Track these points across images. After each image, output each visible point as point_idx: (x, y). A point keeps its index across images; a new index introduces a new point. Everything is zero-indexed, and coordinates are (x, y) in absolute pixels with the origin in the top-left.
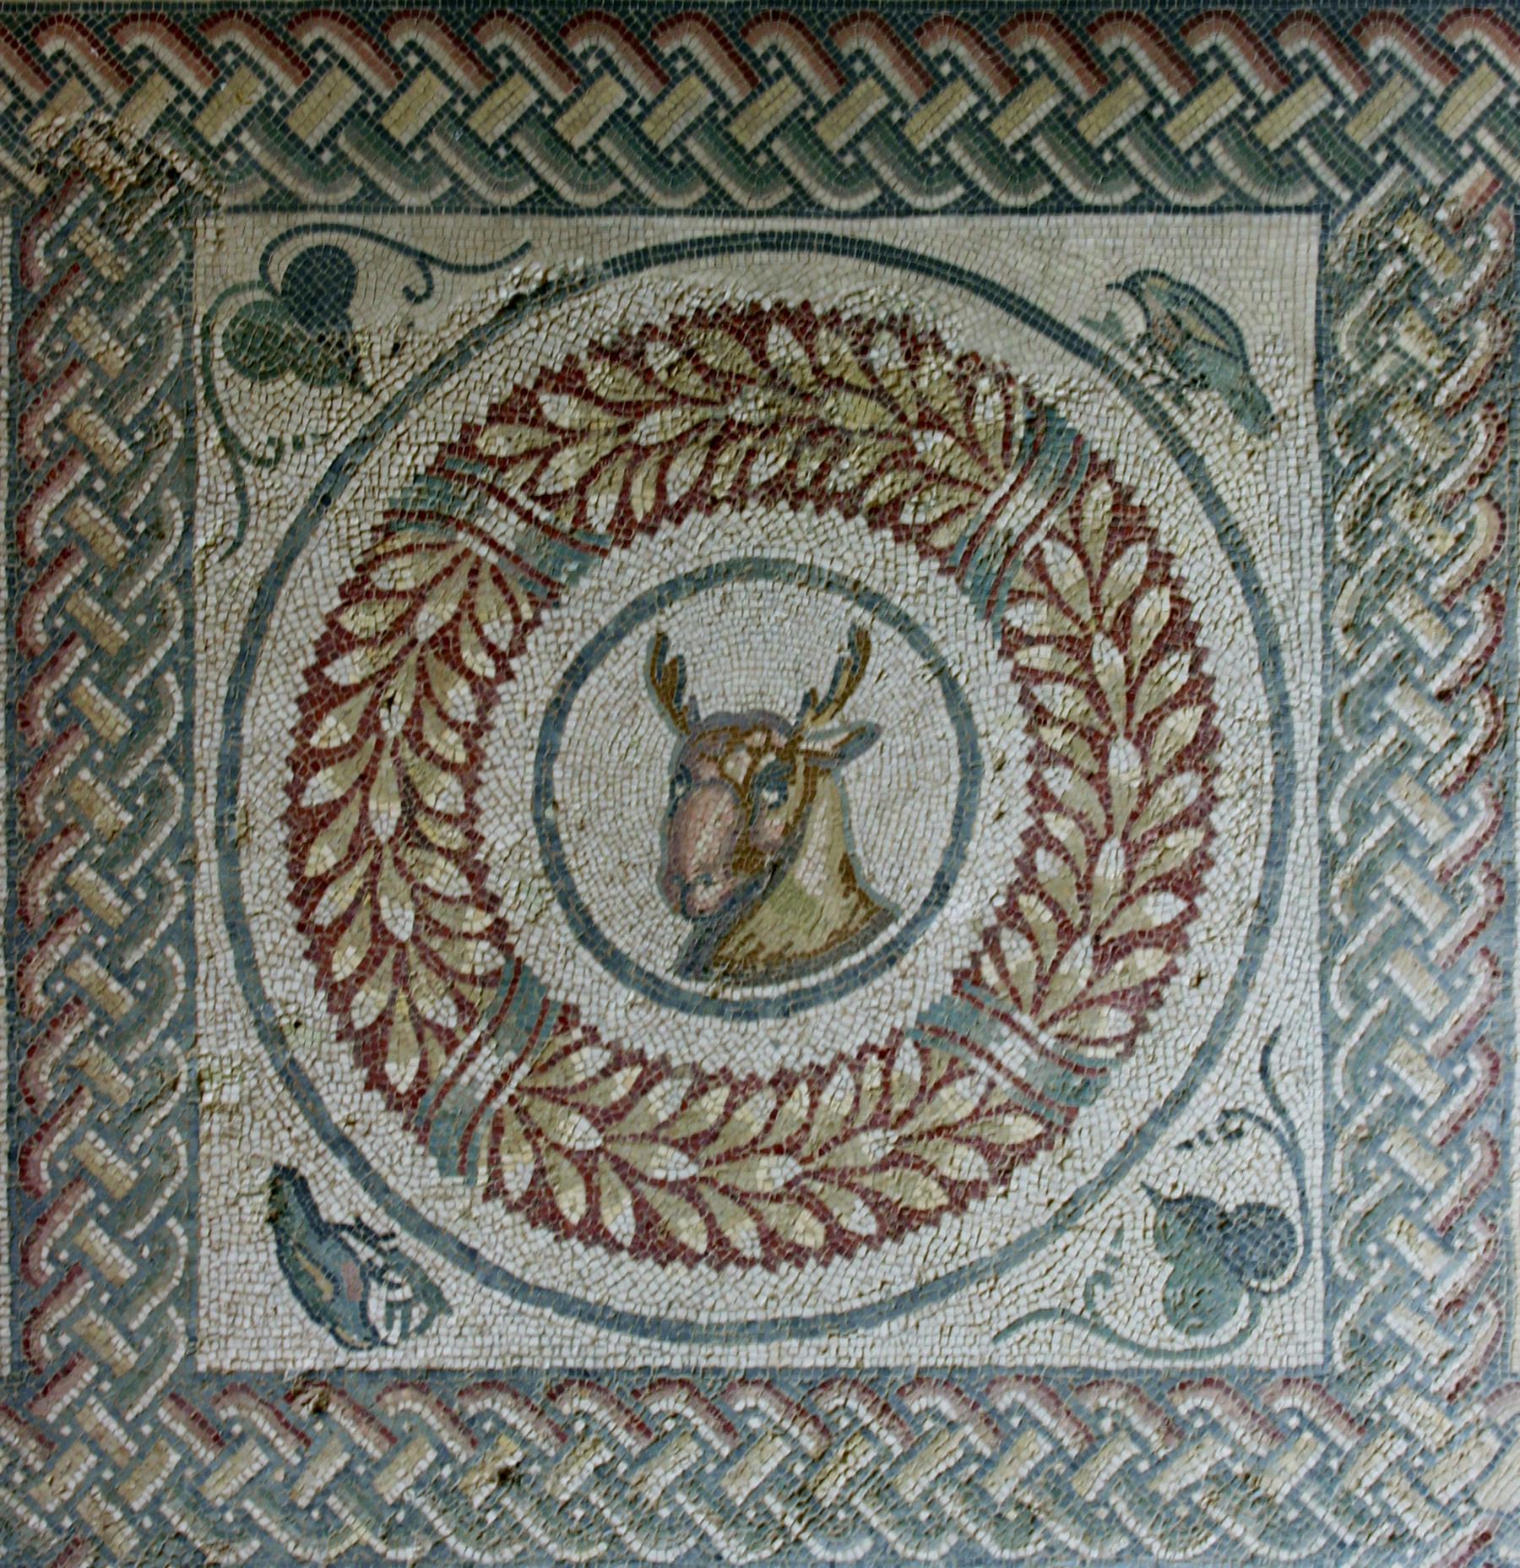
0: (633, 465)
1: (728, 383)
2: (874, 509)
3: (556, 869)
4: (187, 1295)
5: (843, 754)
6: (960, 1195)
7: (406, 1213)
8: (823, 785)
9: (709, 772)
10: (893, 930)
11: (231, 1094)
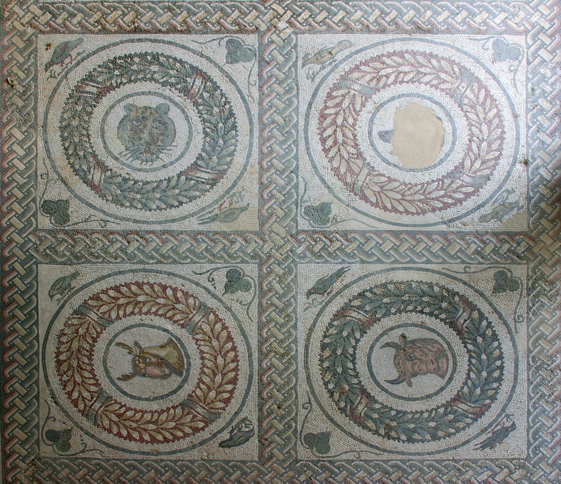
0: (86, 383)
1: (70, 367)
2: (93, 341)
3: (162, 397)
4: (244, 462)
5: (140, 347)
6: (224, 327)
7: (228, 424)
8: (146, 351)
10: (173, 339)
11: (205, 454)
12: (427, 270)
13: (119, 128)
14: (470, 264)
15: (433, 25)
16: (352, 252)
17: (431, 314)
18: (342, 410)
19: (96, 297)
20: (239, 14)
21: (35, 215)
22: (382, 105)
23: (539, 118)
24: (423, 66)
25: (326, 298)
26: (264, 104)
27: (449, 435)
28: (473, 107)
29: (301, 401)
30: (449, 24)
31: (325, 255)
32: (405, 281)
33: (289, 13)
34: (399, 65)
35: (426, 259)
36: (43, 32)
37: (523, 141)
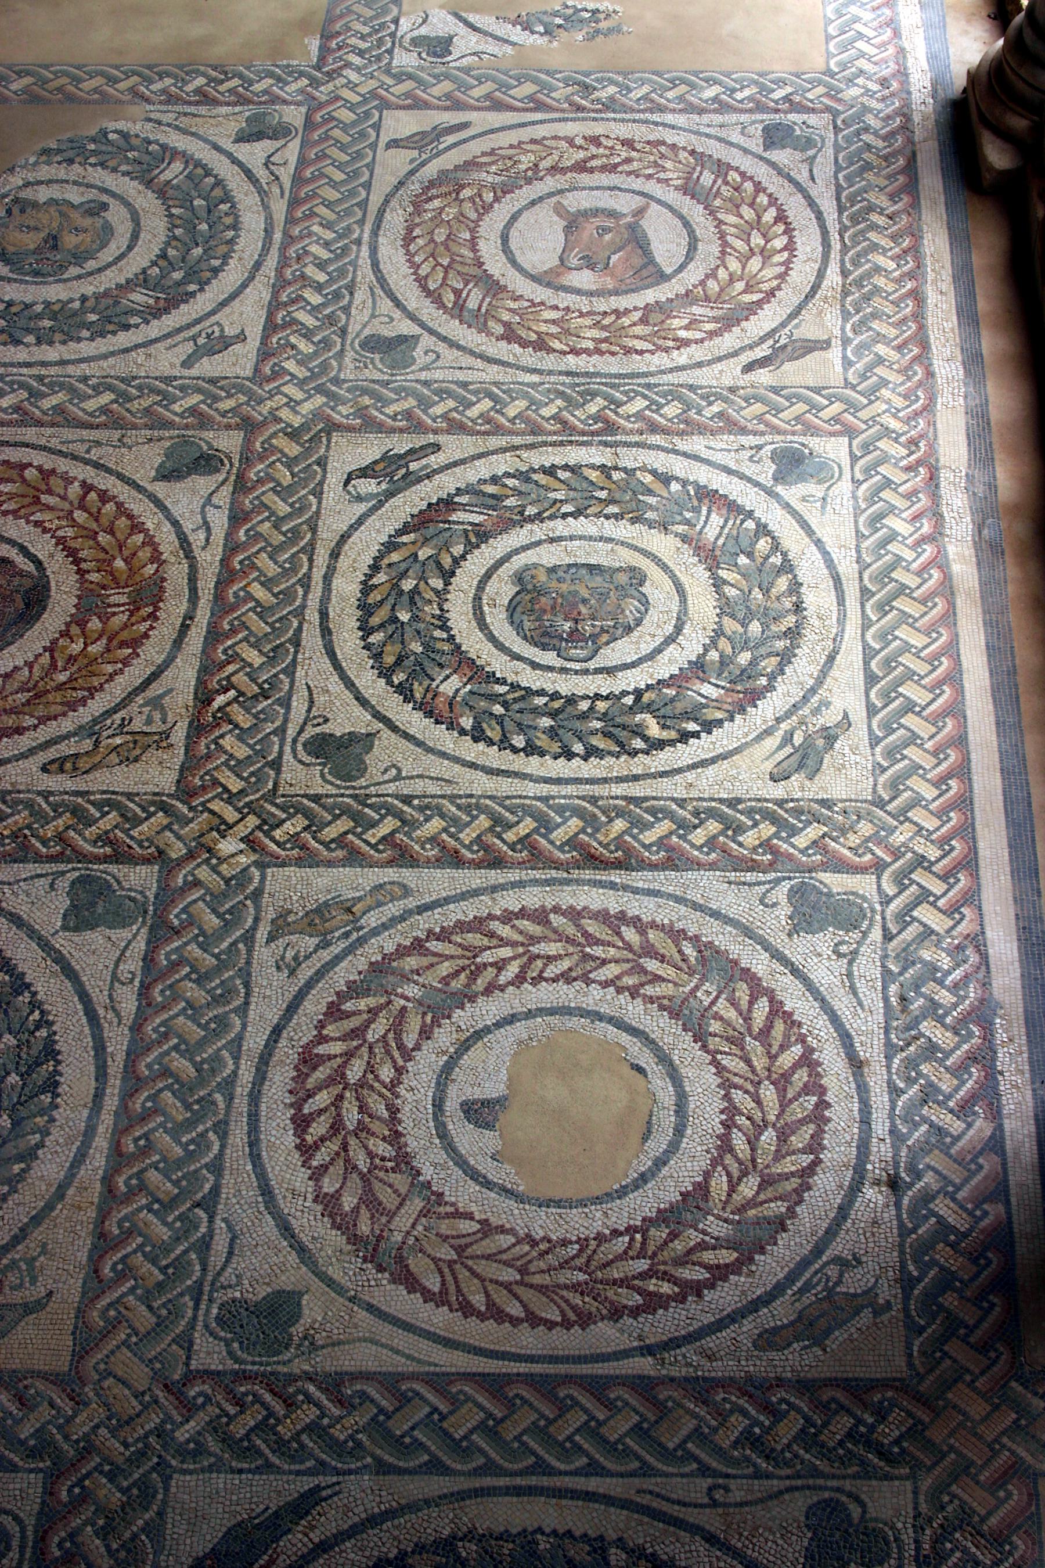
12: (589, 1496)
14: (727, 1476)
15: (628, 851)
16: (351, 1437)
20: (119, 819)
22: (479, 1035)
23: (925, 1068)
24: (598, 942)
28: (737, 1041)
30: (671, 849)
31: (263, 1446)
32: (514, 1531)
34: (534, 940)
35: (585, 1460)
37: (880, 1127)
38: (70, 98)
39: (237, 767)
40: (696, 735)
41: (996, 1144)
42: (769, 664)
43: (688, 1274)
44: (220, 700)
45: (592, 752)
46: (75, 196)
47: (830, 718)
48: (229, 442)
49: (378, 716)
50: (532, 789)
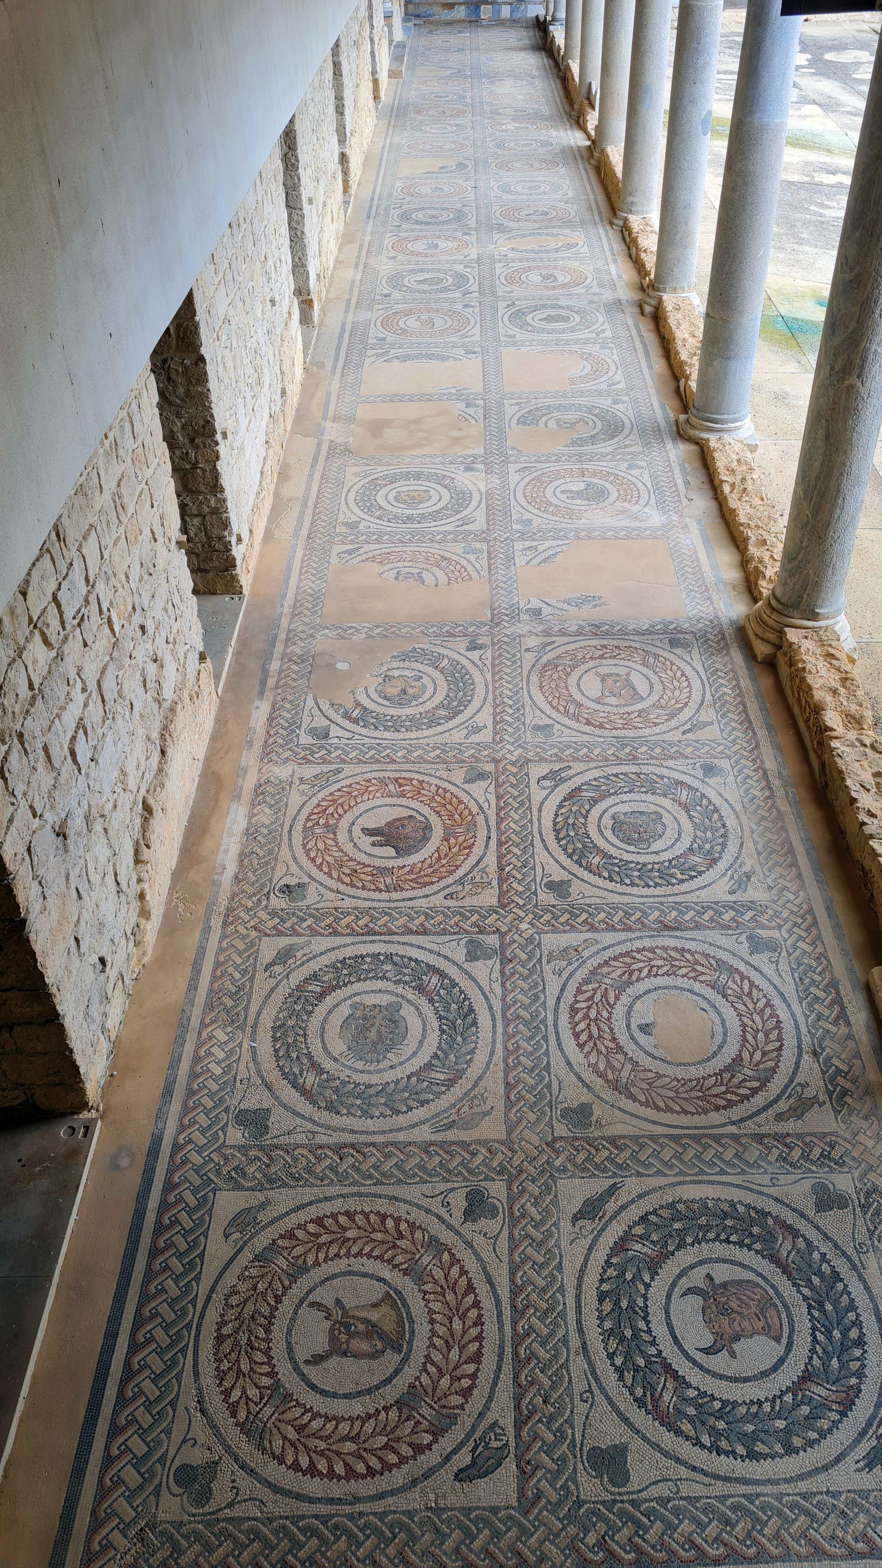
0: (255, 1372)
1: (236, 1343)
2: (276, 1302)
3: (369, 1391)
4: (494, 1510)
5: (343, 1308)
6: (463, 1272)
7: (468, 1436)
9: (345, 1346)
11: (432, 1497)
13: (341, 1027)
17: (740, 1244)
18: (640, 1402)
19: (290, 1235)
21: (223, 1128)
25: (598, 1224)
26: (508, 999)
27: (811, 1443)
29: (577, 1389)
30: (696, 922)
33: (531, 916)
36: (266, 935)
37: (804, 1030)
38: (398, 635)
39: (520, 894)
40: (696, 877)
41: (850, 1037)
42: (718, 848)
43: (742, 1091)
44: (507, 869)
45: (656, 885)
46: (408, 673)
47: (746, 868)
48: (489, 767)
49: (570, 873)
50: (637, 900)
